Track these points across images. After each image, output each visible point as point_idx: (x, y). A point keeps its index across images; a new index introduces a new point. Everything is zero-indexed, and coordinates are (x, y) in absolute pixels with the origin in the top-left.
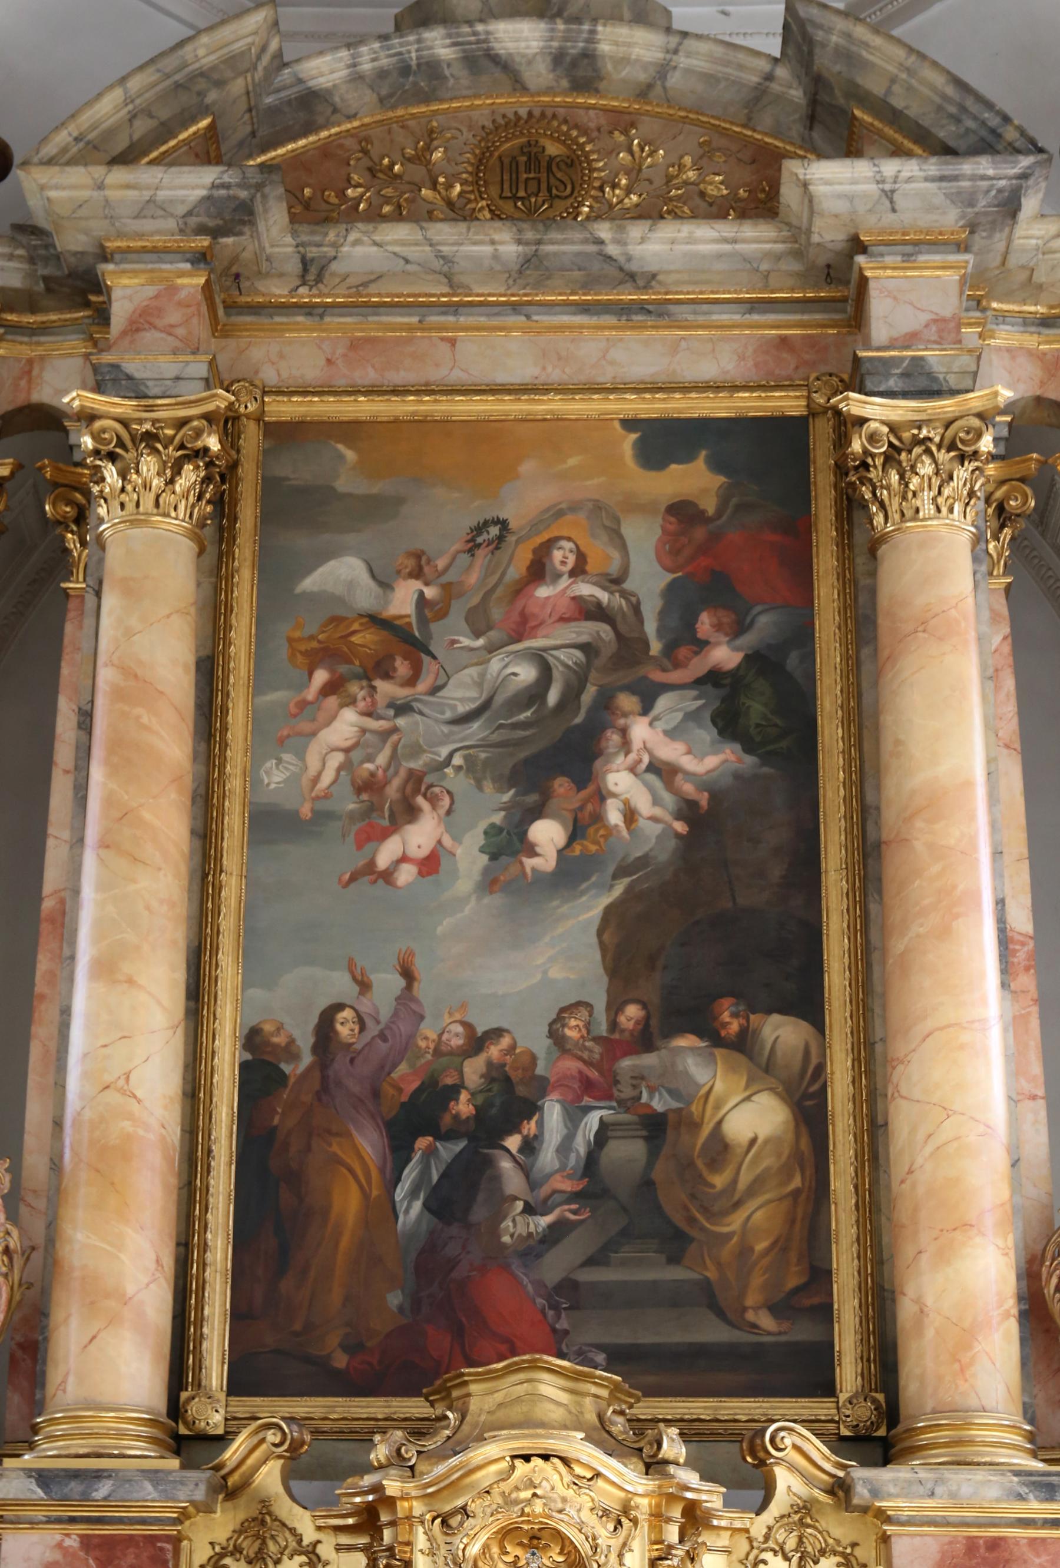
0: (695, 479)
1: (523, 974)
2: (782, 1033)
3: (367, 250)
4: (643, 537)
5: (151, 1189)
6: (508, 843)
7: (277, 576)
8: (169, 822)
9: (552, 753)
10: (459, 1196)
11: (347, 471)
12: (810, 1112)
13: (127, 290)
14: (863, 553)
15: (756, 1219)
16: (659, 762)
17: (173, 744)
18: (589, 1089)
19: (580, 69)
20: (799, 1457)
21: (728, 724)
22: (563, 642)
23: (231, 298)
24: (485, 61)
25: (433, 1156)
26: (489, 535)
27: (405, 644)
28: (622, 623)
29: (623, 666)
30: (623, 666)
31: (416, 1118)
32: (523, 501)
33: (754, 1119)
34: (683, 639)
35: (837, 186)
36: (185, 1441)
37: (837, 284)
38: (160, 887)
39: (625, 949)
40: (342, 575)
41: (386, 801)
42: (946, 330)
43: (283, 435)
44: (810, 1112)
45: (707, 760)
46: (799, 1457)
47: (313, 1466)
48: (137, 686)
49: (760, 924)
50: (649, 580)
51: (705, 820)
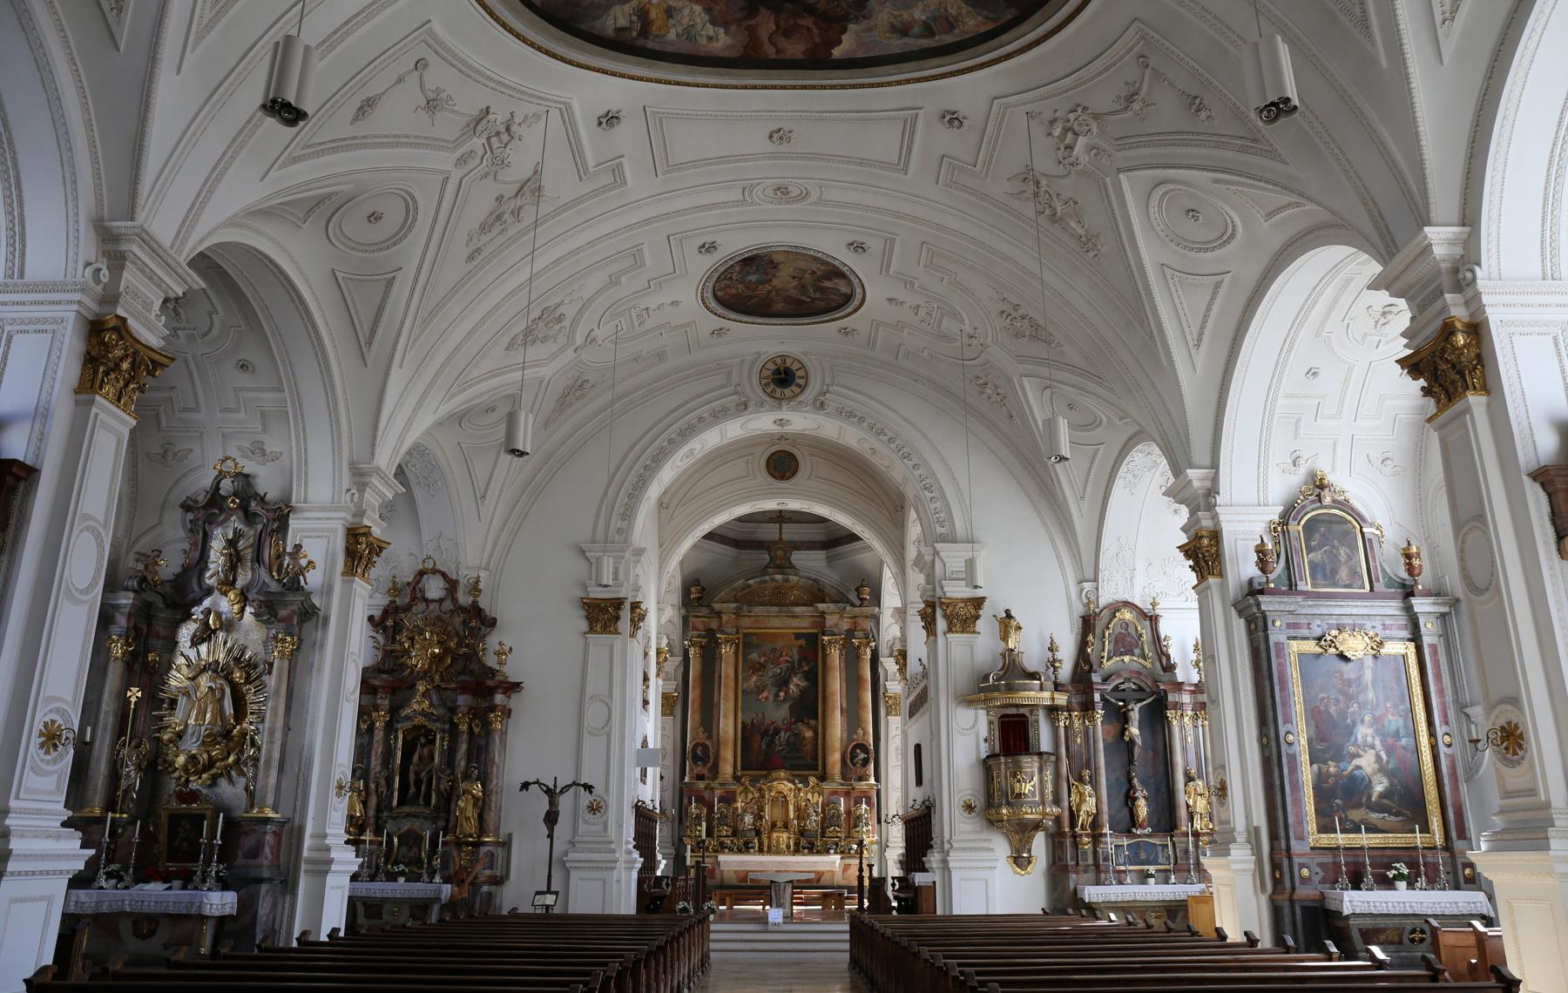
0: (802, 642)
1: (778, 714)
2: (812, 722)
3: (758, 610)
4: (795, 651)
5: (731, 745)
6: (777, 695)
7: (745, 656)
8: (732, 695)
9: (783, 683)
10: (771, 744)
11: (755, 640)
12: (816, 733)
13: (725, 617)
14: (825, 657)
15: (809, 747)
16: (797, 684)
17: (732, 685)
18: (787, 730)
19: (787, 581)
20: (812, 780)
21: (807, 679)
22: (784, 666)
23: (738, 614)
24: (773, 580)
25: (767, 739)
26: (774, 650)
27: (762, 666)
28: (792, 663)
29: (792, 670)
30: (792, 670)
31: (765, 734)
32: (779, 645)
33: (809, 734)
34: (800, 666)
35: (821, 606)
36: (736, 778)
37: (822, 615)
38: (731, 705)
39: (792, 710)
40: (754, 656)
41: (760, 689)
42: (836, 625)
43: (745, 635)
44: (816, 733)
45: (803, 684)
46: (812, 780)
47: (754, 781)
48: (727, 676)
49: (810, 707)
50: (796, 657)
51: (803, 692)
